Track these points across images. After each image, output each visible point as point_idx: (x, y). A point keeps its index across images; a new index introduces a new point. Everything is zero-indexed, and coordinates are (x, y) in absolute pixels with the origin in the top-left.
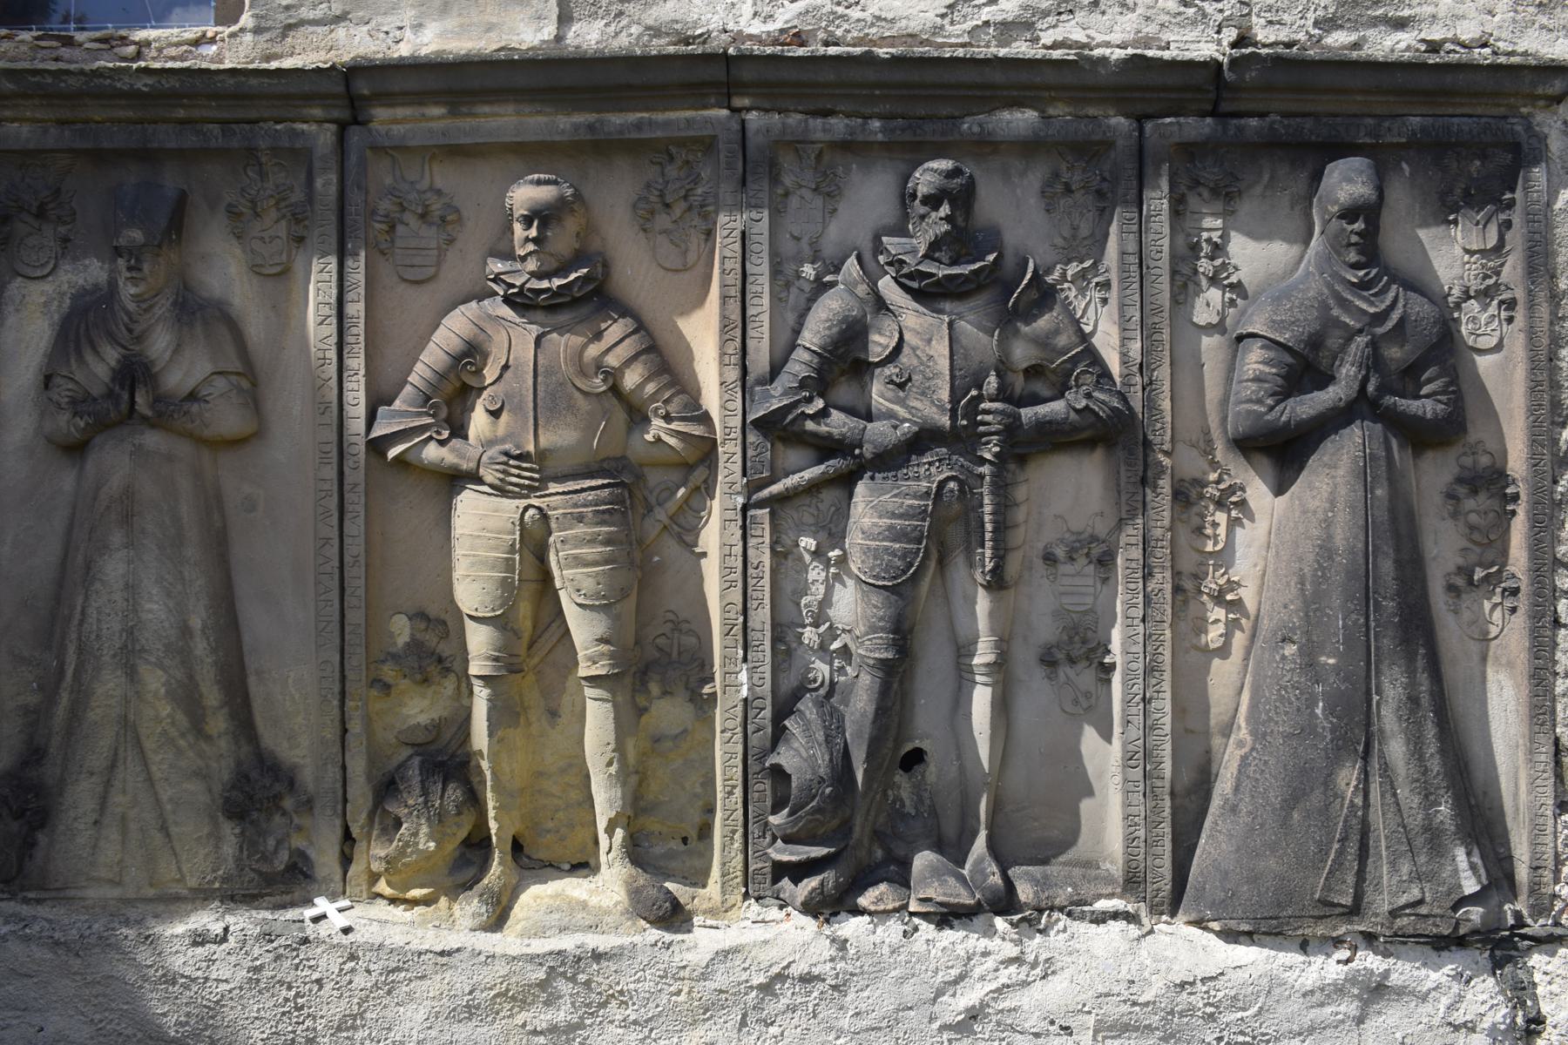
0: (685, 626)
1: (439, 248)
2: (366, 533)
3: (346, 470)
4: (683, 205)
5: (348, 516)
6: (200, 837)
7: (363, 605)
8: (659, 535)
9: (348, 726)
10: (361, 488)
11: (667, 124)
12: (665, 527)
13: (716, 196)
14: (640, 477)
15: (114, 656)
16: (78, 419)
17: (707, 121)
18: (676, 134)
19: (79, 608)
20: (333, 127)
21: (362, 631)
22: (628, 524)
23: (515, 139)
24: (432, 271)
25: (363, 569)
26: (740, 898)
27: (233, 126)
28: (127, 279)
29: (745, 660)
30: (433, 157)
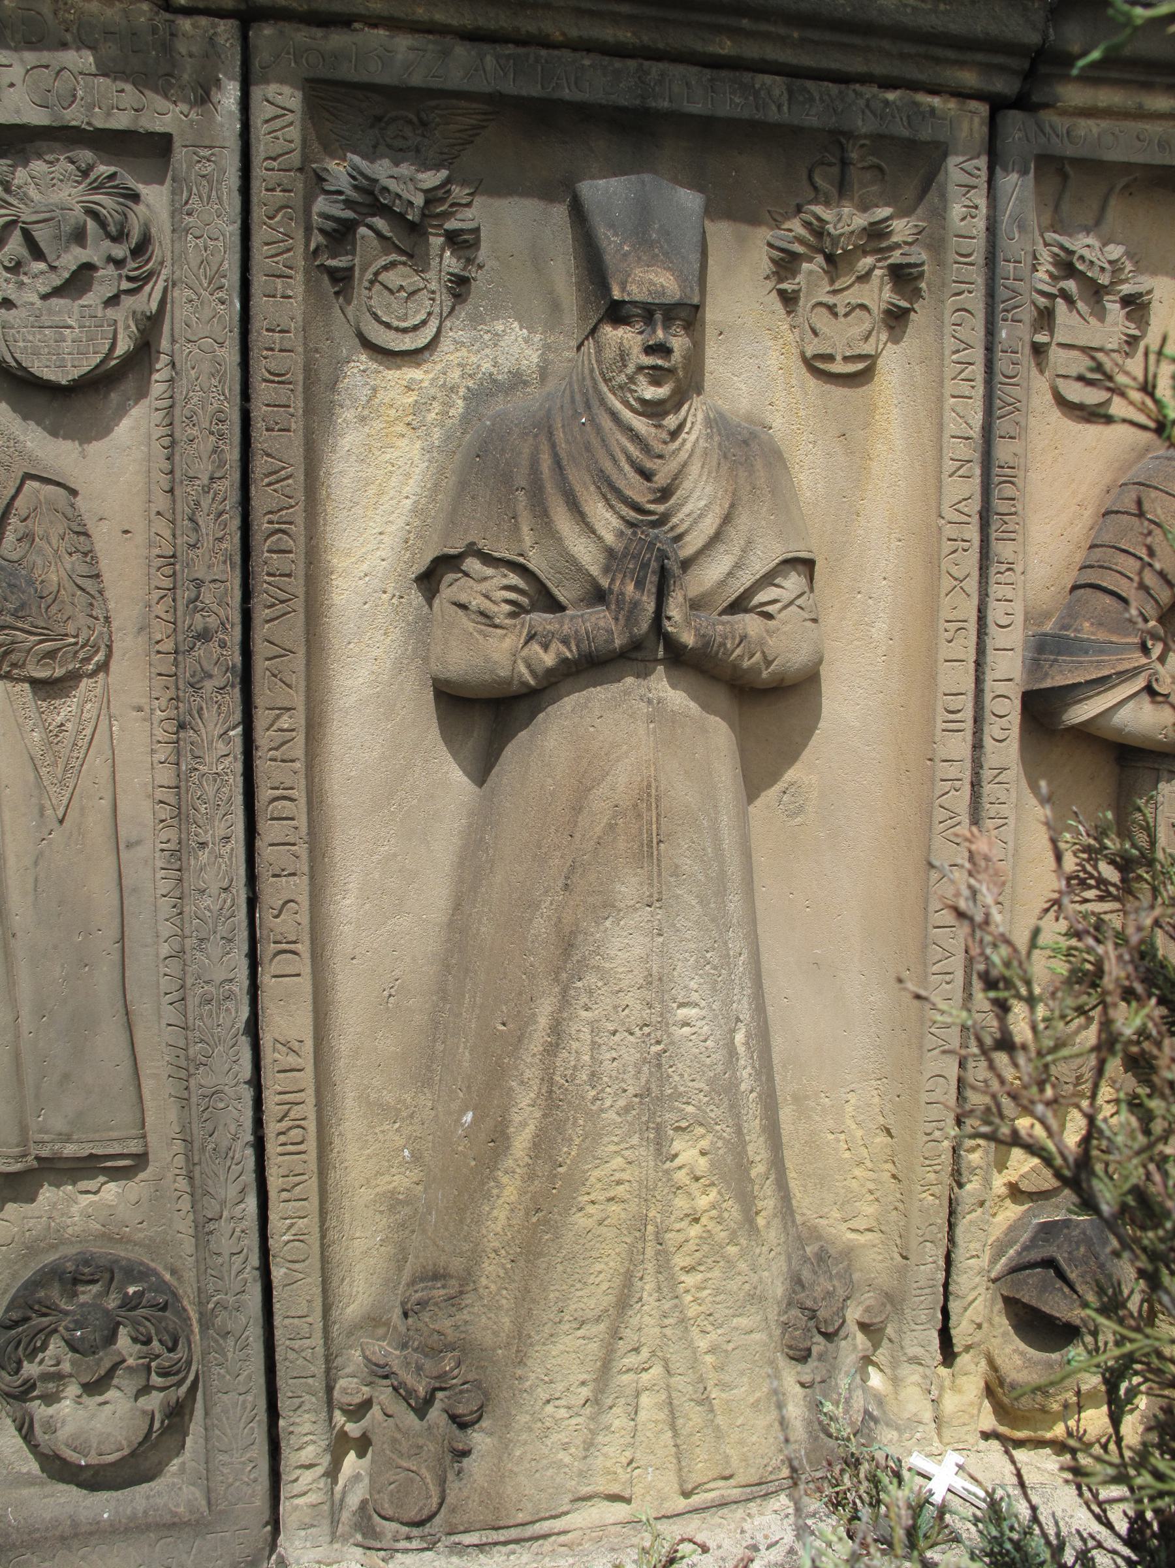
6: (758, 1400)
15: (627, 1109)
16: (535, 647)
19: (543, 1021)
20: (983, 109)
27: (809, 84)
28: (640, 368)
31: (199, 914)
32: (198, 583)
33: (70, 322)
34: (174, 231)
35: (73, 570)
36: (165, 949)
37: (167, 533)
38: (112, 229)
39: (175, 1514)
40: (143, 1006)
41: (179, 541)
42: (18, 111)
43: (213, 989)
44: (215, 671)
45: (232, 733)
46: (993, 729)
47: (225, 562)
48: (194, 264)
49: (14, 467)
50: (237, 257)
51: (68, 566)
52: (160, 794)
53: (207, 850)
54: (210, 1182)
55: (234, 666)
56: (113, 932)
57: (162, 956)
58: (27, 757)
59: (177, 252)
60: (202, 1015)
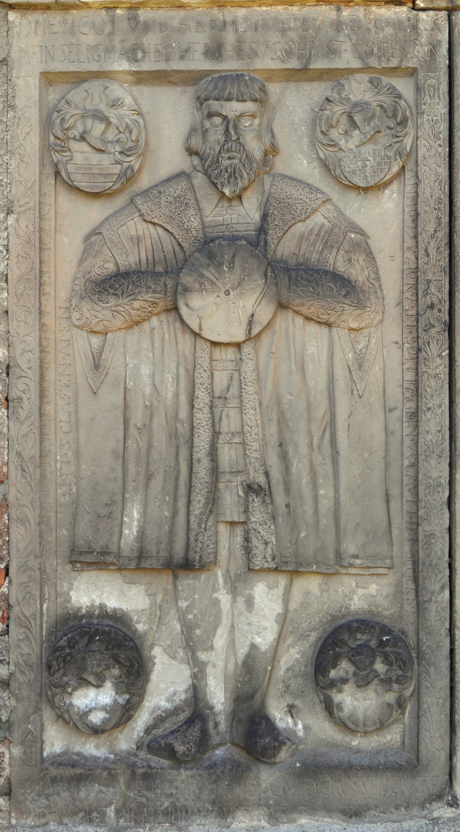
31: (426, 443)
32: (429, 282)
33: (369, 158)
34: (417, 113)
35: (369, 276)
36: (406, 463)
37: (412, 258)
38: (390, 114)
39: (401, 765)
40: (395, 491)
41: (420, 262)
42: (348, 62)
43: (431, 481)
44: (436, 324)
45: (443, 354)
47: (441, 271)
48: (427, 129)
49: (343, 227)
50: (447, 124)
51: (367, 274)
52: (406, 385)
53: (430, 411)
54: (427, 582)
55: (445, 321)
56: (382, 453)
57: (405, 465)
58: (346, 366)
59: (419, 124)
60: (426, 494)
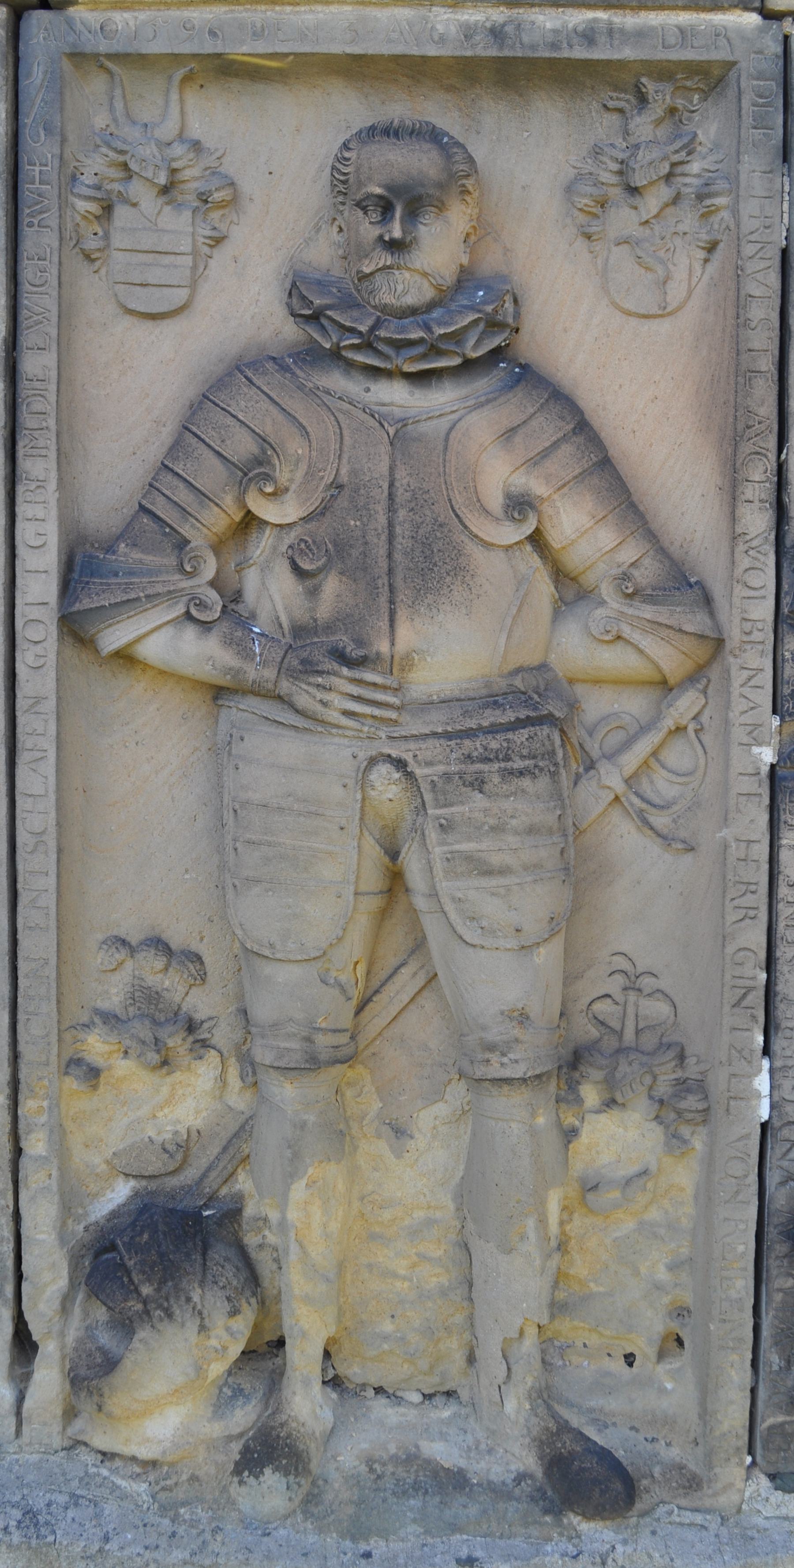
0: (647, 982)
1: (195, 253)
2: (59, 789)
3: (20, 668)
4: (665, 193)
5: (23, 759)
7: (53, 924)
8: (603, 813)
9: (23, 1144)
10: (51, 704)
11: (641, 35)
12: (617, 798)
13: (734, 179)
14: (573, 706)
17: (719, 33)
18: (661, 55)
21: (51, 972)
22: (560, 798)
23: (349, 50)
24: (182, 295)
25: (54, 857)
26: (741, 1472)
29: (766, 1051)
30: (187, 79)
46: (25, 659)
